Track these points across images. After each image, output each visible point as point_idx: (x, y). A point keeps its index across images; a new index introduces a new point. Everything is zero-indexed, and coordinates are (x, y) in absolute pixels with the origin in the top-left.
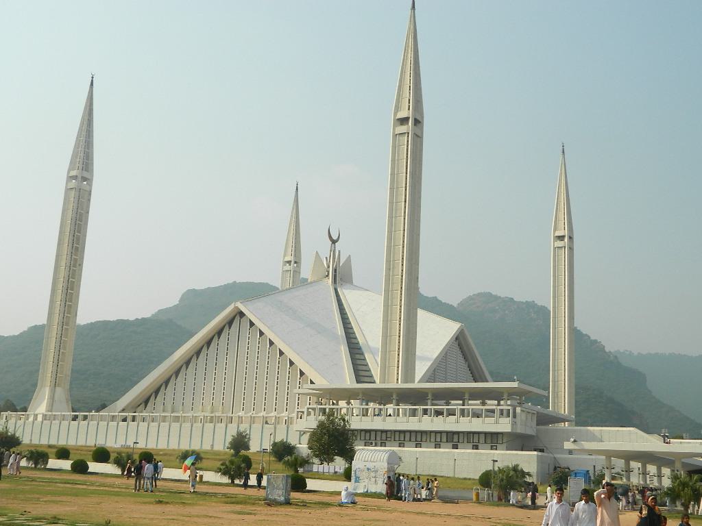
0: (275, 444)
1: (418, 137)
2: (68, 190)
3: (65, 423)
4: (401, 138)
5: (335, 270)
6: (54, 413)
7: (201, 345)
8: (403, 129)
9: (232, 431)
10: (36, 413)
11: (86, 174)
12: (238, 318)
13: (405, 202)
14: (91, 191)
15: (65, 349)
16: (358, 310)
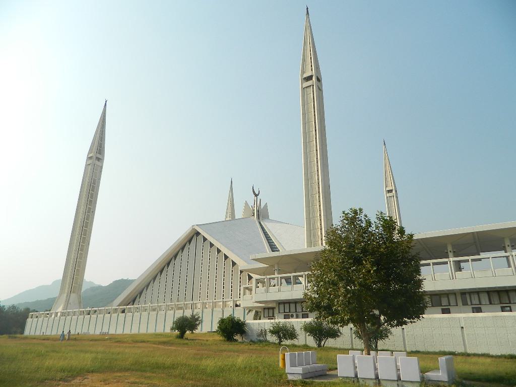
0: (222, 321)
1: (320, 89)
2: (87, 165)
3: (69, 318)
4: (308, 89)
5: (258, 211)
6: (68, 311)
7: (170, 258)
8: (309, 83)
9: (188, 314)
10: (57, 312)
11: (99, 156)
12: (195, 237)
13: (316, 131)
14: (102, 167)
15: (79, 266)
16: (275, 233)
